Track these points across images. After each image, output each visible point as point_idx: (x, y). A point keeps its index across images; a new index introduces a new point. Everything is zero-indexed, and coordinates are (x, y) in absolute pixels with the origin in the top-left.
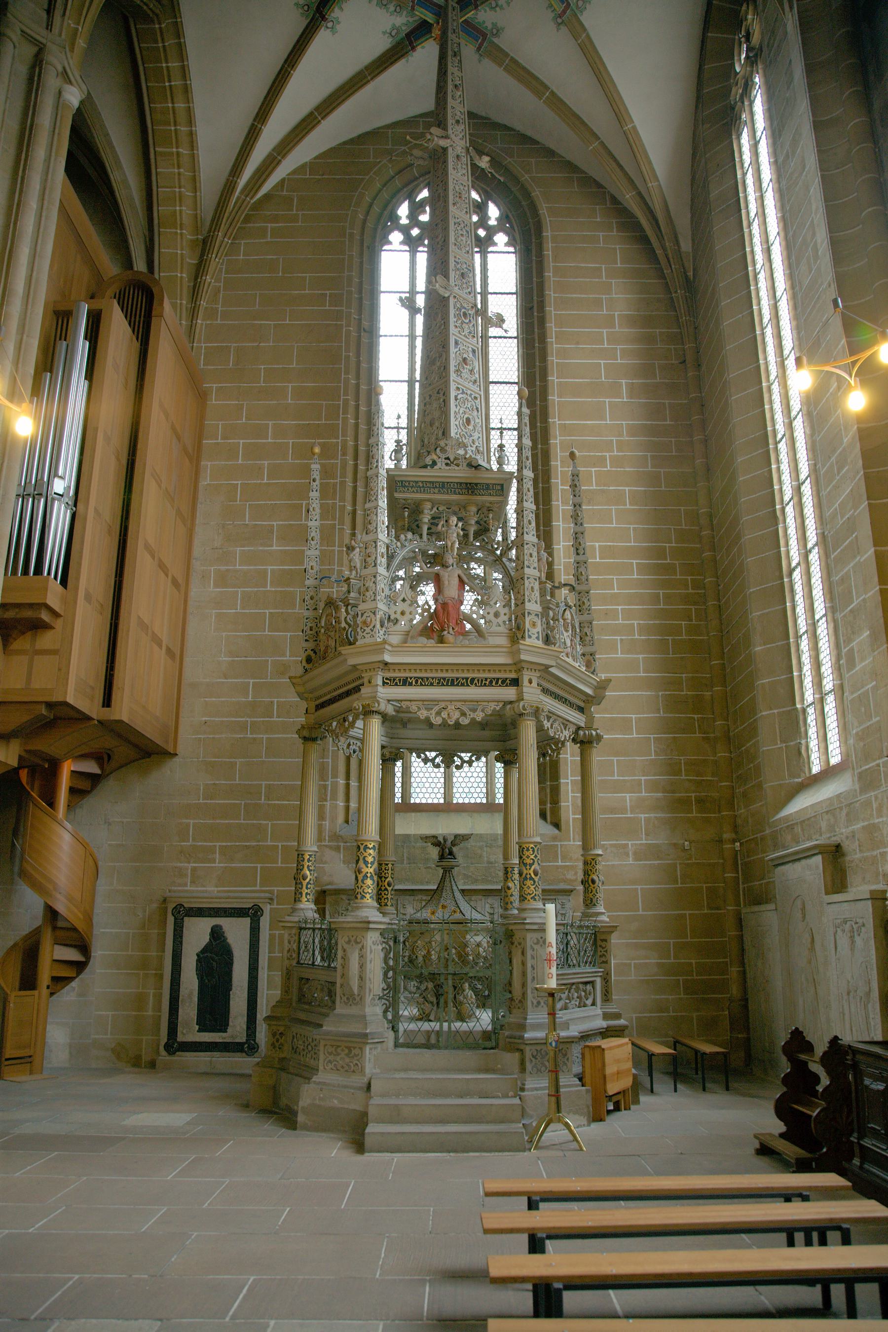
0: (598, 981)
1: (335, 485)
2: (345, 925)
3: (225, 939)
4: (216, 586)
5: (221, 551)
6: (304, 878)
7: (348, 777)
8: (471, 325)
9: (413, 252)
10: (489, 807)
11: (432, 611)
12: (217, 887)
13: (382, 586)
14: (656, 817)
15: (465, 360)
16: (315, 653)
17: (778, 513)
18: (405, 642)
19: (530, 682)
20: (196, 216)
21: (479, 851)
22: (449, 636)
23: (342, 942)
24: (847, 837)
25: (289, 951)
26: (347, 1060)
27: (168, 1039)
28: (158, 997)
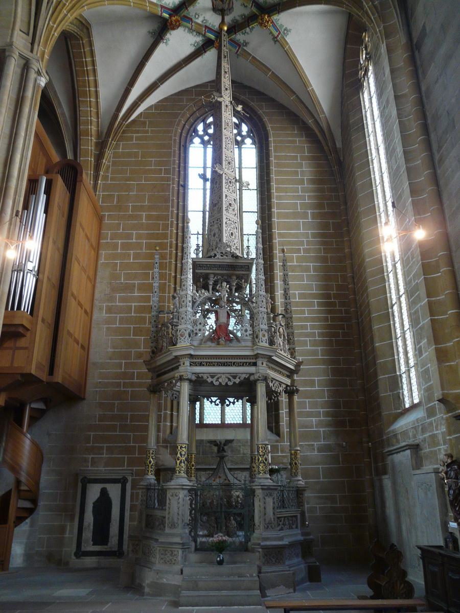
0: (299, 515)
1: (166, 263)
2: (171, 487)
3: (108, 495)
4: (106, 313)
5: (109, 296)
6: (150, 462)
7: (172, 410)
8: (233, 187)
9: (205, 148)
10: (243, 425)
11: (214, 329)
12: (104, 467)
13: (190, 317)
14: (328, 430)
15: (230, 204)
16: (156, 349)
17: (386, 277)
18: (201, 344)
20: (98, 130)
21: (239, 449)
22: (222, 341)
23: (169, 495)
24: (422, 441)
25: (142, 500)
26: (171, 558)
27: (77, 550)
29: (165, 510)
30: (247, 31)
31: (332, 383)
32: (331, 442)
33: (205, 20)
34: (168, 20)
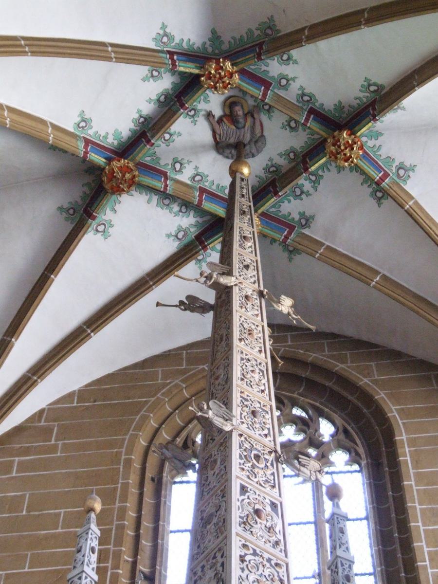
8: (269, 472)
30: (305, 189)
33: (197, 175)
34: (104, 169)
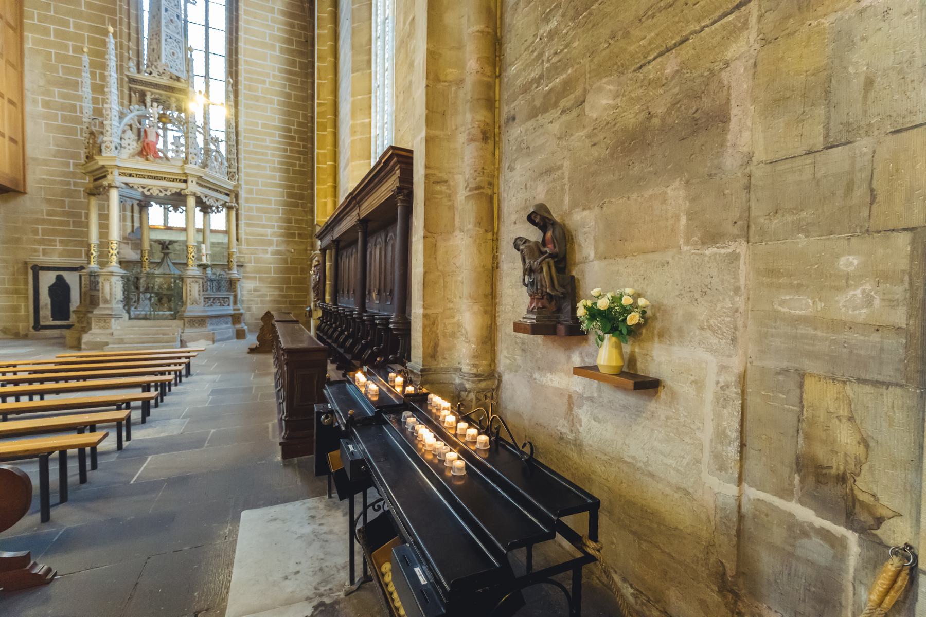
0: (232, 298)
6: (92, 254)
12: (59, 257)
15: (171, 20)
19: (192, 182)
22: (150, 157)
28: (27, 307)
29: (98, 290)
31: (287, 204)
32: (282, 248)
